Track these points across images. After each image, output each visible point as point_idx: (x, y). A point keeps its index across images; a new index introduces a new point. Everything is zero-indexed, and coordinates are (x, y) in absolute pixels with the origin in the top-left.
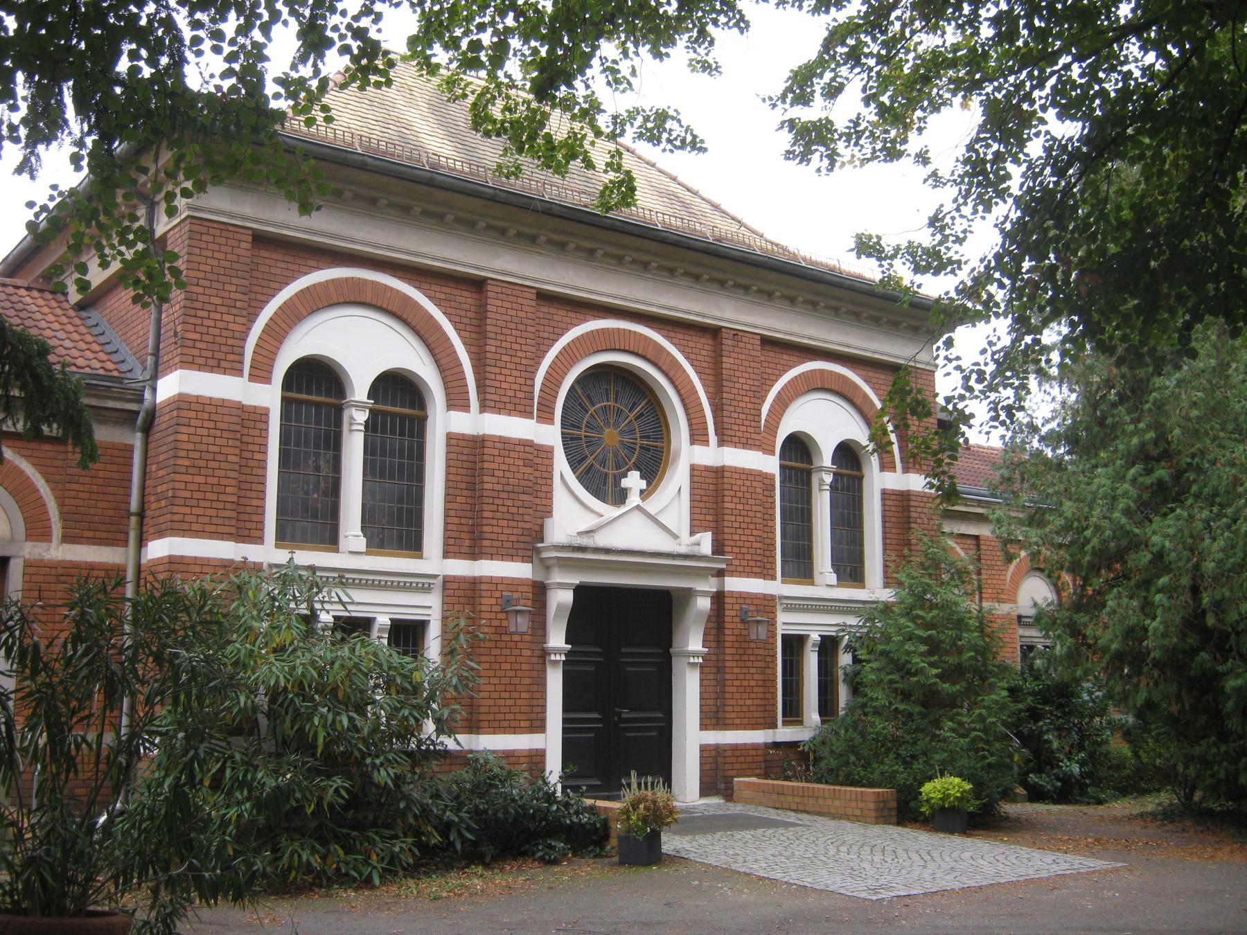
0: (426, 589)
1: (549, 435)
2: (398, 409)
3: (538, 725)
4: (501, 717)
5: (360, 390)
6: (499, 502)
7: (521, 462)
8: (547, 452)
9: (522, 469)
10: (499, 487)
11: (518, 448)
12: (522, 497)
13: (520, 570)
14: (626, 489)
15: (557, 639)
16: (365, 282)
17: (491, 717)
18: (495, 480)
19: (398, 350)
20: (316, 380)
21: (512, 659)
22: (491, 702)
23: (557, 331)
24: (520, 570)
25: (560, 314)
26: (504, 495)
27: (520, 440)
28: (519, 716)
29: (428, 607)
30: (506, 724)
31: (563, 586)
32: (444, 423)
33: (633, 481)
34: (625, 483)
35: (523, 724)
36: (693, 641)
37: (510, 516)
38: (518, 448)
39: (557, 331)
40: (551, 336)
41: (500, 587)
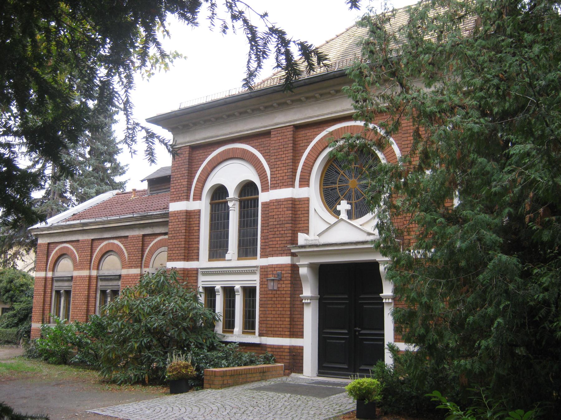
0: (254, 273)
1: (312, 193)
2: (249, 197)
3: (300, 335)
4: (277, 329)
5: (232, 193)
6: (276, 230)
7: (285, 209)
8: (307, 201)
9: (286, 212)
10: (276, 223)
11: (284, 203)
12: (286, 225)
13: (285, 260)
14: (340, 211)
15: (308, 291)
16: (230, 149)
17: (272, 329)
18: (274, 220)
19: (248, 173)
20: (220, 192)
21: (281, 302)
22: (272, 322)
23: (308, 141)
24: (285, 260)
25: (309, 132)
26: (278, 226)
27: (285, 199)
28: (285, 330)
29: (254, 280)
30: (279, 333)
31: (303, 266)
32: (264, 197)
33: (344, 206)
34: (339, 208)
35: (286, 333)
36: (388, 290)
37: (280, 236)
38: (284, 203)
39: (308, 141)
40: (306, 144)
41: (276, 269)
